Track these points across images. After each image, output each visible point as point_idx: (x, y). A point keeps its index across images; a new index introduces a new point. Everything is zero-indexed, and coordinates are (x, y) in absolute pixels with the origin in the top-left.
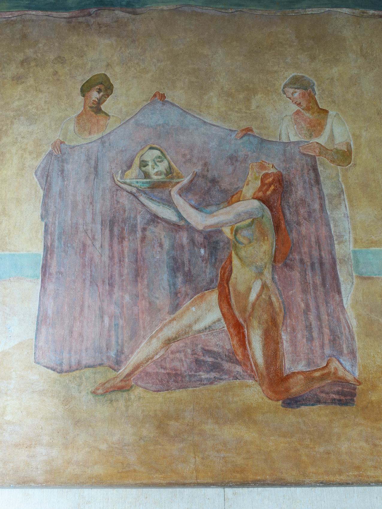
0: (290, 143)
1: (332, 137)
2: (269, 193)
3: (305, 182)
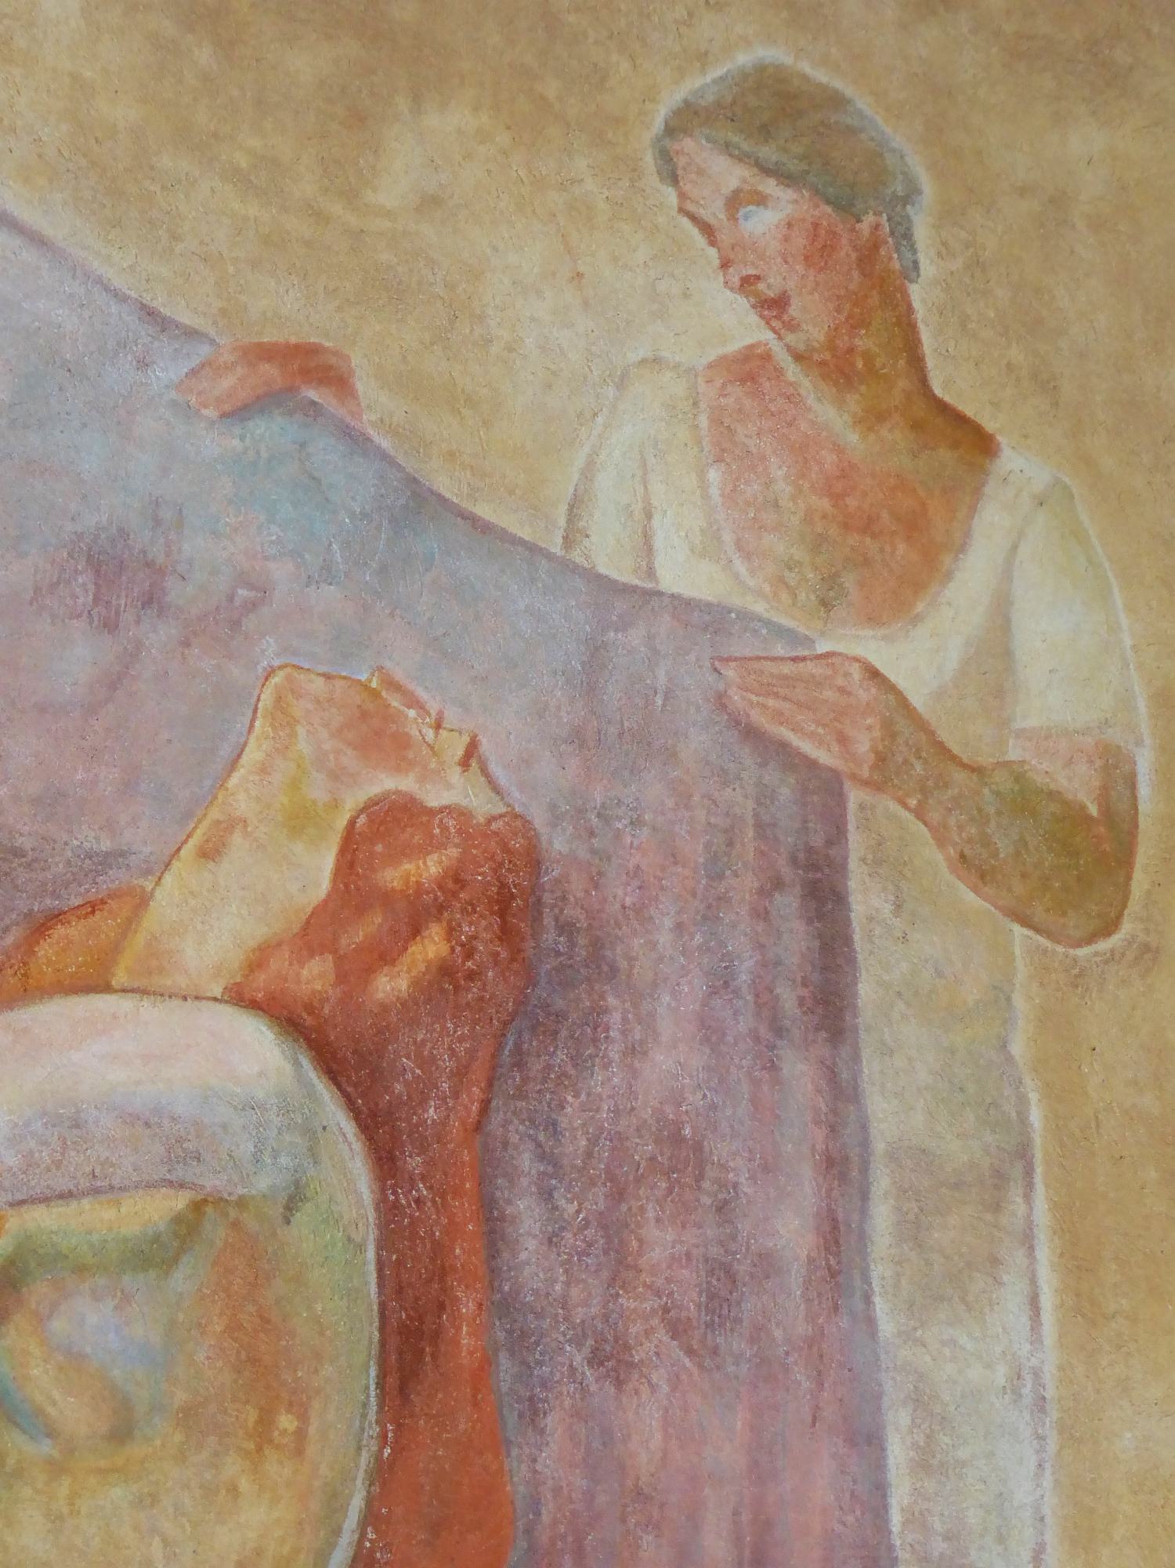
0: (649, 596)
1: (994, 656)
2: (390, 985)
3: (722, 983)
